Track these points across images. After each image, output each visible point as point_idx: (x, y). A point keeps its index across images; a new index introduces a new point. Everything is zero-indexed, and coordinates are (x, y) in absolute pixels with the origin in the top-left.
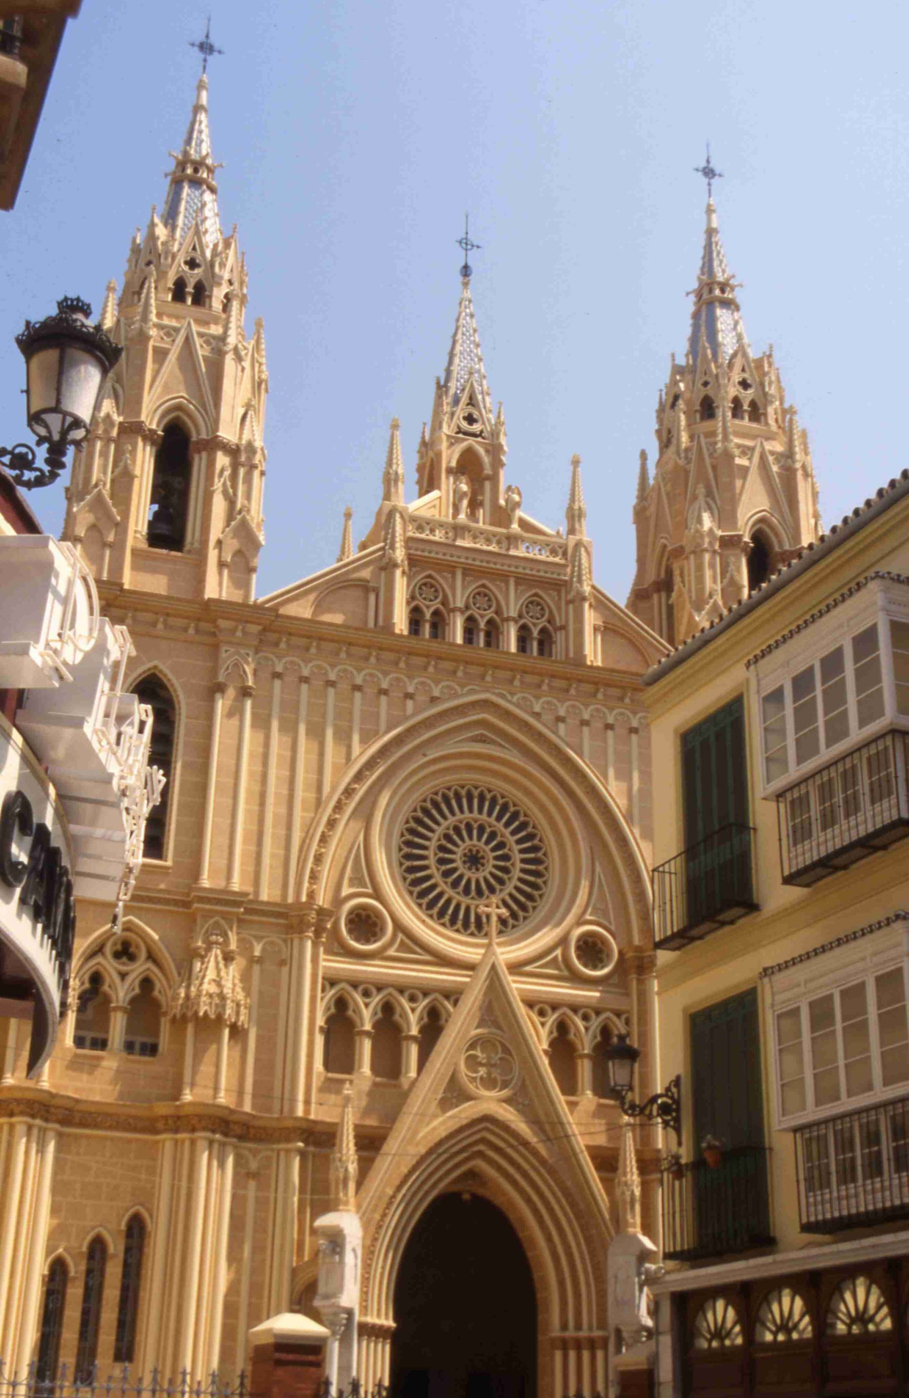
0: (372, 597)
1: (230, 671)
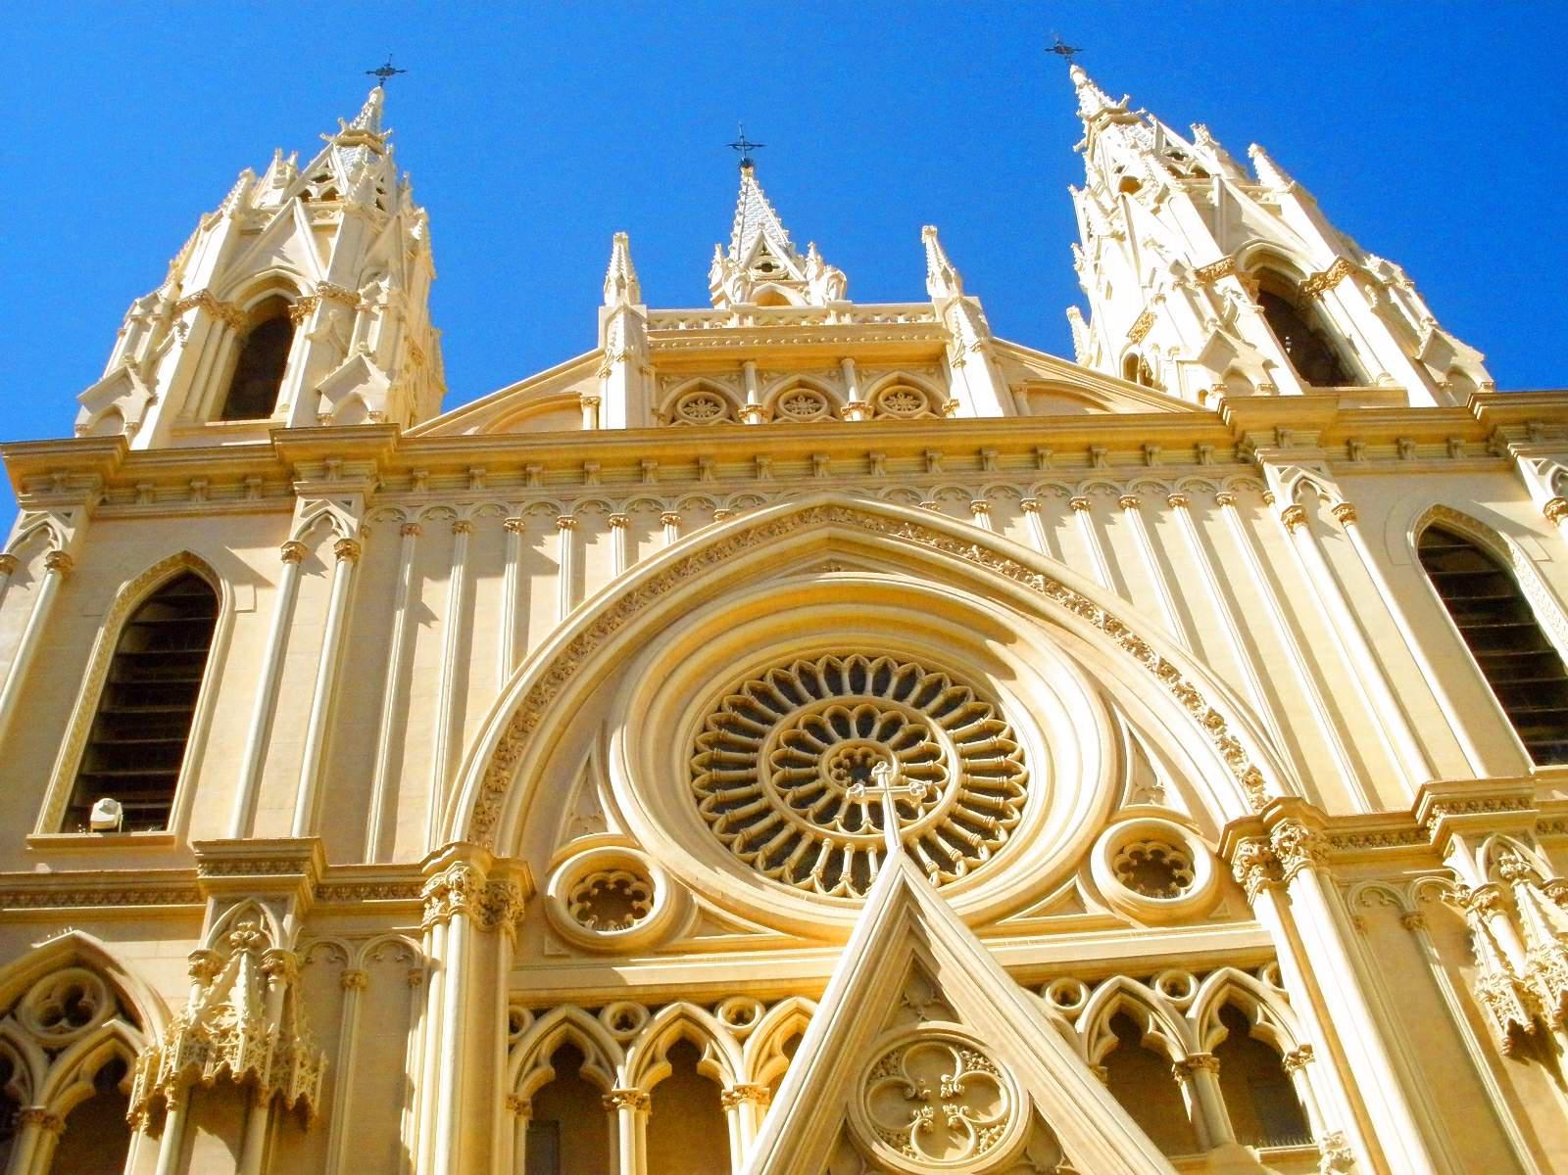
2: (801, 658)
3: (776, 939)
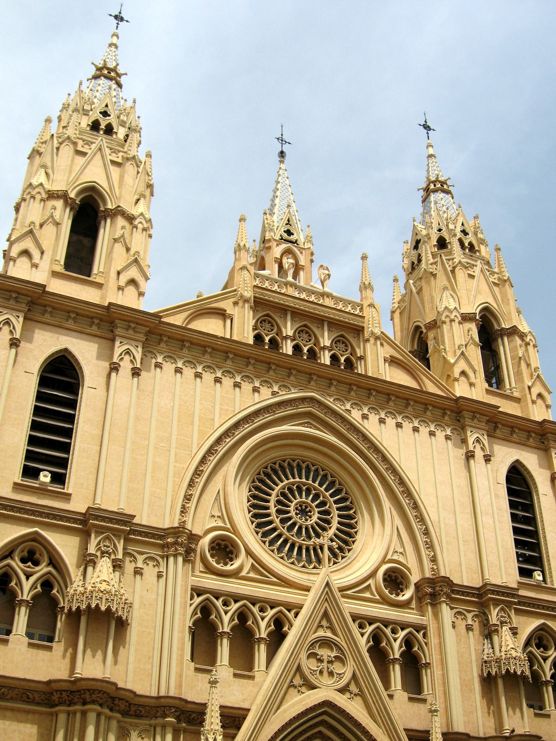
0: (228, 322)
1: (123, 356)
2: (290, 458)
3: (275, 582)
